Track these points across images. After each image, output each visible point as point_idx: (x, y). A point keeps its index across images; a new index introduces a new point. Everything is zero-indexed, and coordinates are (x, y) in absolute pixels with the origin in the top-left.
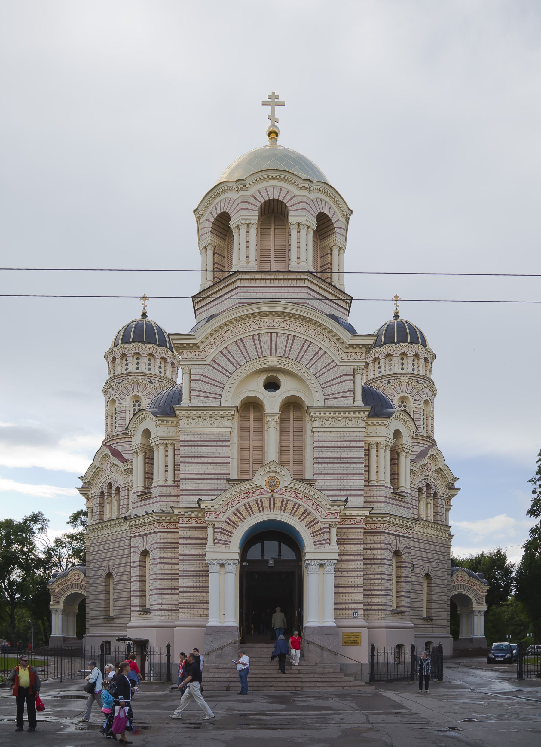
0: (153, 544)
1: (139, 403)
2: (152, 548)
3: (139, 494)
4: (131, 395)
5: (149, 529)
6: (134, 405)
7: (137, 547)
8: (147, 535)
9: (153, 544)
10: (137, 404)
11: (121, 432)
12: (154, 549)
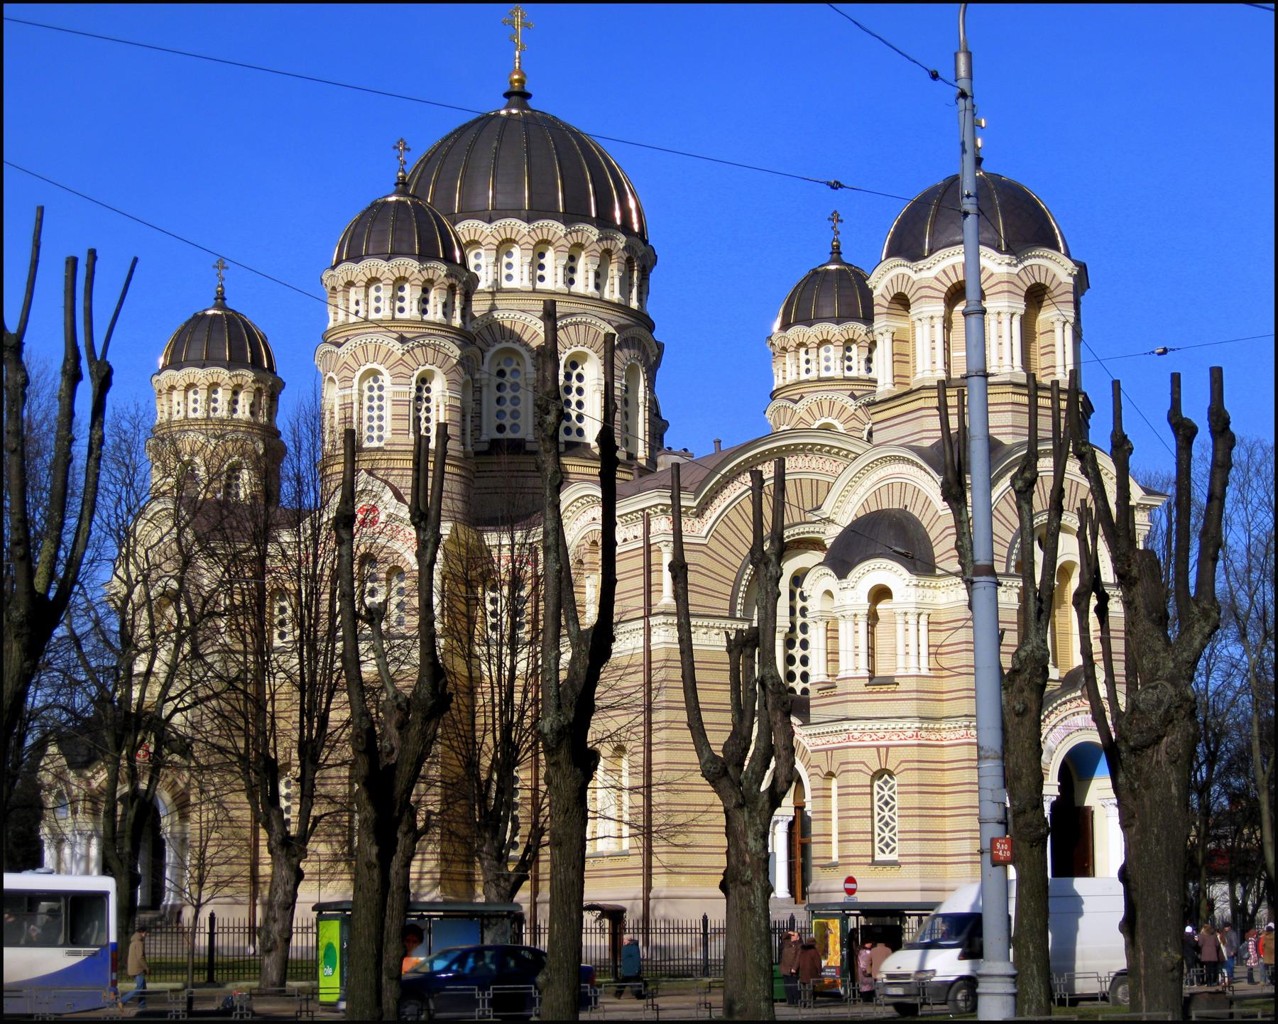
7: (863, 763)
8: (888, 747)
9: (902, 762)
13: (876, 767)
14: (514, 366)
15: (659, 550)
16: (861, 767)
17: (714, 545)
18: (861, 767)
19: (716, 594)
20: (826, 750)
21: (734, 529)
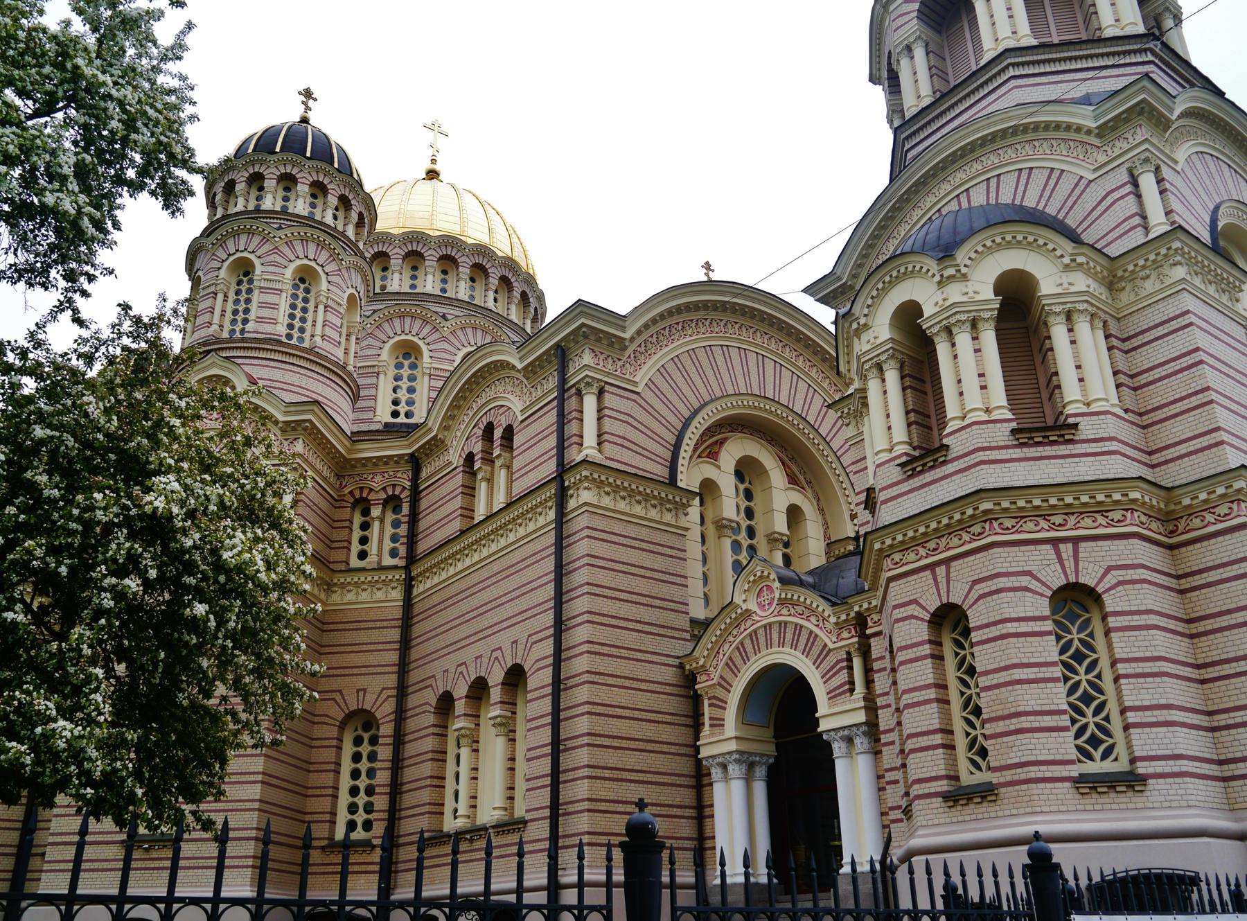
0: (1109, 569)
1: (307, 285)
3: (1014, 425)
4: (298, 262)
5: (1088, 527)
6: (296, 287)
7: (1029, 573)
8: (1076, 541)
9: (1109, 569)
10: (302, 286)
11: (264, 336)
12: (1120, 583)
13: (1058, 581)
14: (412, 360)
15: (579, 394)
16: (1025, 581)
17: (648, 395)
18: (1025, 581)
20: (931, 567)
21: (673, 385)
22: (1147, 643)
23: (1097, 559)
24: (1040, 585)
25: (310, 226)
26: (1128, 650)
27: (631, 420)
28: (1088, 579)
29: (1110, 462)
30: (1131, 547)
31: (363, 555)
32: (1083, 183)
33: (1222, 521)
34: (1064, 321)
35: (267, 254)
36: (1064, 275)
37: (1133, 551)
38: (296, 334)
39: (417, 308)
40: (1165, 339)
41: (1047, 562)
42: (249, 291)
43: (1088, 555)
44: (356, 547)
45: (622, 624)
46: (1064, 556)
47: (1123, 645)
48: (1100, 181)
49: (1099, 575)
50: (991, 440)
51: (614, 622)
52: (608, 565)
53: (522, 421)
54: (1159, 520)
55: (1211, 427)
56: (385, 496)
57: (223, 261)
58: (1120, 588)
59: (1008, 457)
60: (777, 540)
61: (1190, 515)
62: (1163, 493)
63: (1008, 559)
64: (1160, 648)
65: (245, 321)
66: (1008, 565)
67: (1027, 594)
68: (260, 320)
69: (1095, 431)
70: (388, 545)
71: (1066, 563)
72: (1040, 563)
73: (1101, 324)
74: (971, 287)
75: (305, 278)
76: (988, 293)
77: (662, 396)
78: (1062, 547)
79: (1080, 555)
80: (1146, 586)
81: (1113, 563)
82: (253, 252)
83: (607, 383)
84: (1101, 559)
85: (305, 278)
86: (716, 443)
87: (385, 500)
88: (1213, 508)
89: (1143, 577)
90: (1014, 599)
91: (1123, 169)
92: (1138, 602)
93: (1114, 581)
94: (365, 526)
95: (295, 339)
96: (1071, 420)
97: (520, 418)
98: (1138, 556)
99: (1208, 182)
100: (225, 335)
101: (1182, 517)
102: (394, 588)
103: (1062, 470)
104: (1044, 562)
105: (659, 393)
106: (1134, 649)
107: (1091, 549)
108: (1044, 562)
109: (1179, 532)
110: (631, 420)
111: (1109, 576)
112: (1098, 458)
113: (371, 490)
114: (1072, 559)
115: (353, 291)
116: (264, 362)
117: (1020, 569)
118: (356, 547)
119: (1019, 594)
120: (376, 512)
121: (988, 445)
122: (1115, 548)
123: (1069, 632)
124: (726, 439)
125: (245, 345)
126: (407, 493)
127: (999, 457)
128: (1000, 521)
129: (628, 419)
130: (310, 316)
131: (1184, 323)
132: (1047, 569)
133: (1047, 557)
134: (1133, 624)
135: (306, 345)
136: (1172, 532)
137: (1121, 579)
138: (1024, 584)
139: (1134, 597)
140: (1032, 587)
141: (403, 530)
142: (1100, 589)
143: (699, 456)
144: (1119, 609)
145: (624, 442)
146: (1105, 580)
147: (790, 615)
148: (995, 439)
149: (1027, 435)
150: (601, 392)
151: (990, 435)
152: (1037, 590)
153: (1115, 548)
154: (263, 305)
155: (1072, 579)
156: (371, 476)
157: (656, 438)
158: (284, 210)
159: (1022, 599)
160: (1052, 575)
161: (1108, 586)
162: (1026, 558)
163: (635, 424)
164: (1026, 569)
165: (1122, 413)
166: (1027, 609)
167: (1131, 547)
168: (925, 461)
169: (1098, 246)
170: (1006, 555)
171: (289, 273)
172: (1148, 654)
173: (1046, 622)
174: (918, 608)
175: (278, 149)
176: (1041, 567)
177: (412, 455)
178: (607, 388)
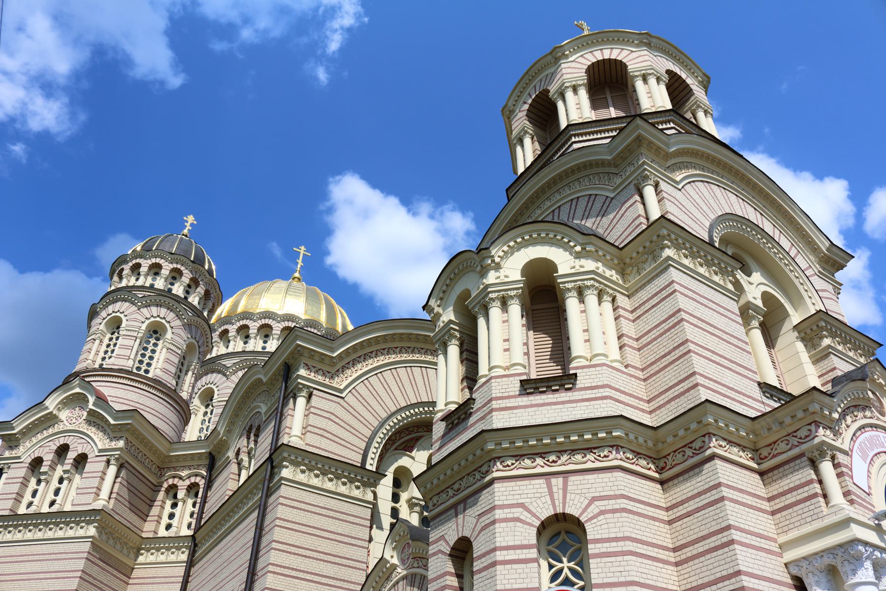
0: (594, 499)
1: (158, 335)
2: (594, 509)
5: (579, 461)
7: (522, 505)
9: (594, 499)
10: (154, 336)
12: (602, 513)
13: (546, 512)
16: (518, 512)
18: (518, 512)
19: (349, 446)
21: (374, 393)
22: (621, 569)
23: (584, 491)
24: (530, 516)
25: (163, 296)
26: (604, 575)
27: (332, 417)
28: (573, 510)
29: (602, 406)
30: (614, 479)
31: (168, 527)
32: (609, 200)
33: (697, 454)
34: (576, 295)
35: (131, 313)
36: (577, 261)
37: (615, 483)
38: (144, 367)
39: (254, 360)
40: (658, 306)
41: (539, 495)
42: (117, 338)
43: (575, 487)
44: (165, 520)
45: (301, 575)
46: (555, 489)
47: (600, 570)
48: (618, 198)
49: (583, 506)
50: (504, 391)
51: (294, 573)
52: (296, 527)
53: (265, 422)
54: (650, 457)
55: (689, 373)
56: (189, 483)
57: (104, 319)
58: (602, 517)
59: (516, 404)
60: (416, 505)
61: (675, 452)
62: (651, 432)
63: (505, 493)
64: (634, 573)
65: (110, 357)
66: (504, 498)
67: (518, 524)
68: (119, 357)
69: (591, 381)
70: (187, 519)
71: (556, 496)
72: (532, 495)
73: (610, 299)
74: (502, 273)
75: (156, 331)
76: (516, 275)
77: (363, 401)
78: (554, 481)
79: (569, 488)
80: (624, 514)
81: (597, 494)
82: (123, 312)
83: (315, 389)
84: (586, 491)
85: (156, 331)
86: (412, 439)
87: (189, 486)
88: (691, 443)
89: (622, 506)
90: (506, 529)
91: (632, 186)
92: (617, 530)
93: (596, 511)
94: (174, 505)
95: (142, 371)
96: (571, 372)
97: (264, 419)
98: (620, 487)
99: (711, 201)
100: (97, 366)
101: (669, 455)
102: (183, 553)
103: (560, 414)
104: (537, 495)
105: (361, 399)
106: (609, 575)
107: (578, 482)
108: (537, 495)
109: (668, 468)
110: (332, 417)
111: (593, 506)
112: (592, 403)
113: (181, 478)
114: (561, 492)
115: (194, 341)
116: (114, 385)
117: (515, 502)
118: (165, 520)
119: (511, 524)
120: (181, 494)
121: (500, 395)
122: (600, 480)
123: (561, 562)
124: (421, 437)
125: (104, 373)
126: (203, 481)
127: (508, 405)
128: (502, 459)
129: (331, 417)
130: (156, 356)
131: (670, 292)
132: (539, 501)
133: (540, 491)
134: (610, 550)
135: (150, 375)
136: (663, 468)
137: (603, 508)
138: (516, 515)
139: (613, 525)
140: (522, 517)
141: (196, 510)
142: (583, 519)
143: (396, 449)
144: (599, 537)
145: (324, 433)
146: (589, 510)
147: (418, 567)
148: (507, 390)
149: (534, 386)
150: (310, 396)
151: (504, 387)
152: (528, 520)
153: (600, 480)
154: (123, 347)
155: (559, 510)
156: (182, 468)
157: (354, 431)
158: (152, 286)
159: (513, 529)
160: (542, 506)
161: (591, 515)
162: (521, 492)
163: (337, 420)
164: (520, 501)
165: (624, 369)
166: (516, 538)
167: (614, 479)
168: (459, 414)
169: (616, 244)
170: (504, 489)
171: (144, 327)
172: (622, 579)
173: (531, 550)
174: (444, 544)
175: (154, 249)
176: (533, 500)
177: (210, 453)
178: (315, 392)
